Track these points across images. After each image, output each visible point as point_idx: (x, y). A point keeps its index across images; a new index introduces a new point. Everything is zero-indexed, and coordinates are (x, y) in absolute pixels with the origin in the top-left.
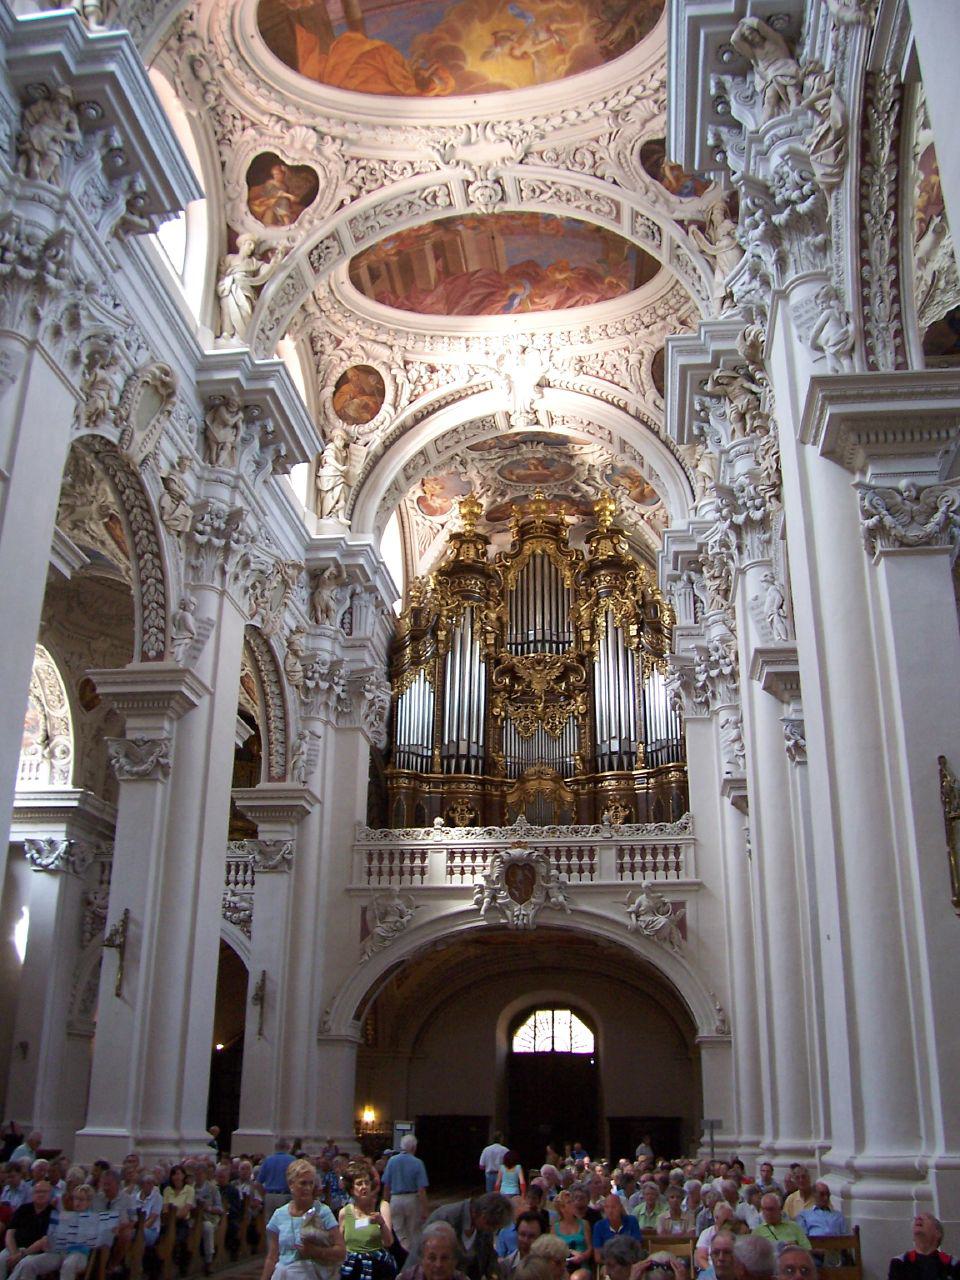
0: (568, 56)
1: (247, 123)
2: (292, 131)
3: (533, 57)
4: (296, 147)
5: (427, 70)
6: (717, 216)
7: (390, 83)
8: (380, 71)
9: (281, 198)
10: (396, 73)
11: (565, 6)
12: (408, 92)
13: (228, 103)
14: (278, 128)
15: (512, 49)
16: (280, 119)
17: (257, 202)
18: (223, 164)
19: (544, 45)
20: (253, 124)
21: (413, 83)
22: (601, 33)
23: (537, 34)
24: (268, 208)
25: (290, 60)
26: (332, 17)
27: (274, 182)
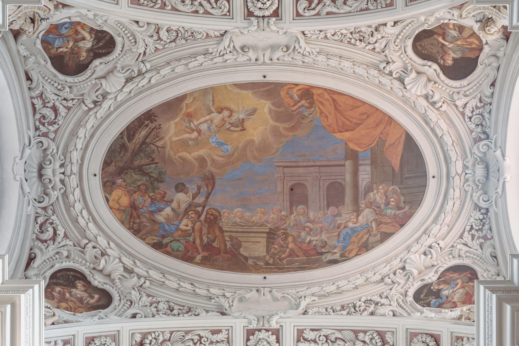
0: (184, 111)
1: (461, 109)
2: (424, 92)
3: (213, 110)
4: (426, 81)
5: (303, 106)
6: (29, 28)
7: (334, 100)
8: (339, 112)
9: (451, 43)
10: (328, 109)
11: (185, 154)
12: (320, 91)
13: (472, 132)
14: (436, 98)
15: (229, 117)
16: (433, 104)
17: (474, 46)
18: (493, 85)
19: (203, 119)
20: (456, 106)
21: (315, 97)
22: (156, 133)
23: (209, 128)
24: (465, 39)
25: (410, 142)
26: (368, 168)
27: (453, 55)
